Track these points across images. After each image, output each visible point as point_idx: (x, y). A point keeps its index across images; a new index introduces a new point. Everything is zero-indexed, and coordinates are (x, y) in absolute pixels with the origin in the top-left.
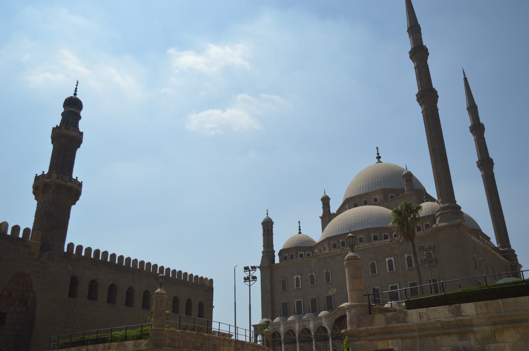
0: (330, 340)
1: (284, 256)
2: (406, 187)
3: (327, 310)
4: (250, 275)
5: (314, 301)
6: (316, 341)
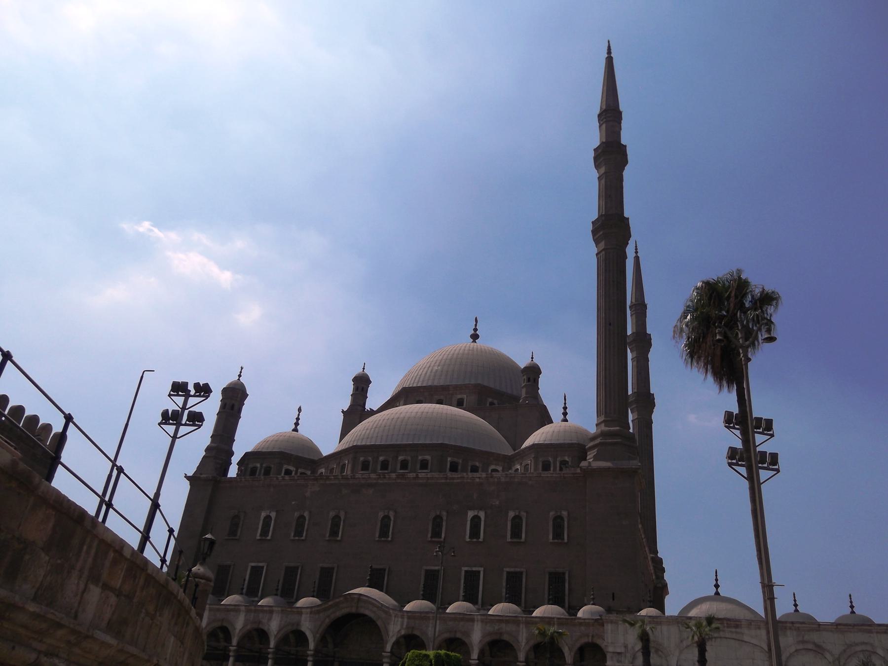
1: (251, 466)
2: (524, 391)
4: (184, 408)
5: (291, 573)
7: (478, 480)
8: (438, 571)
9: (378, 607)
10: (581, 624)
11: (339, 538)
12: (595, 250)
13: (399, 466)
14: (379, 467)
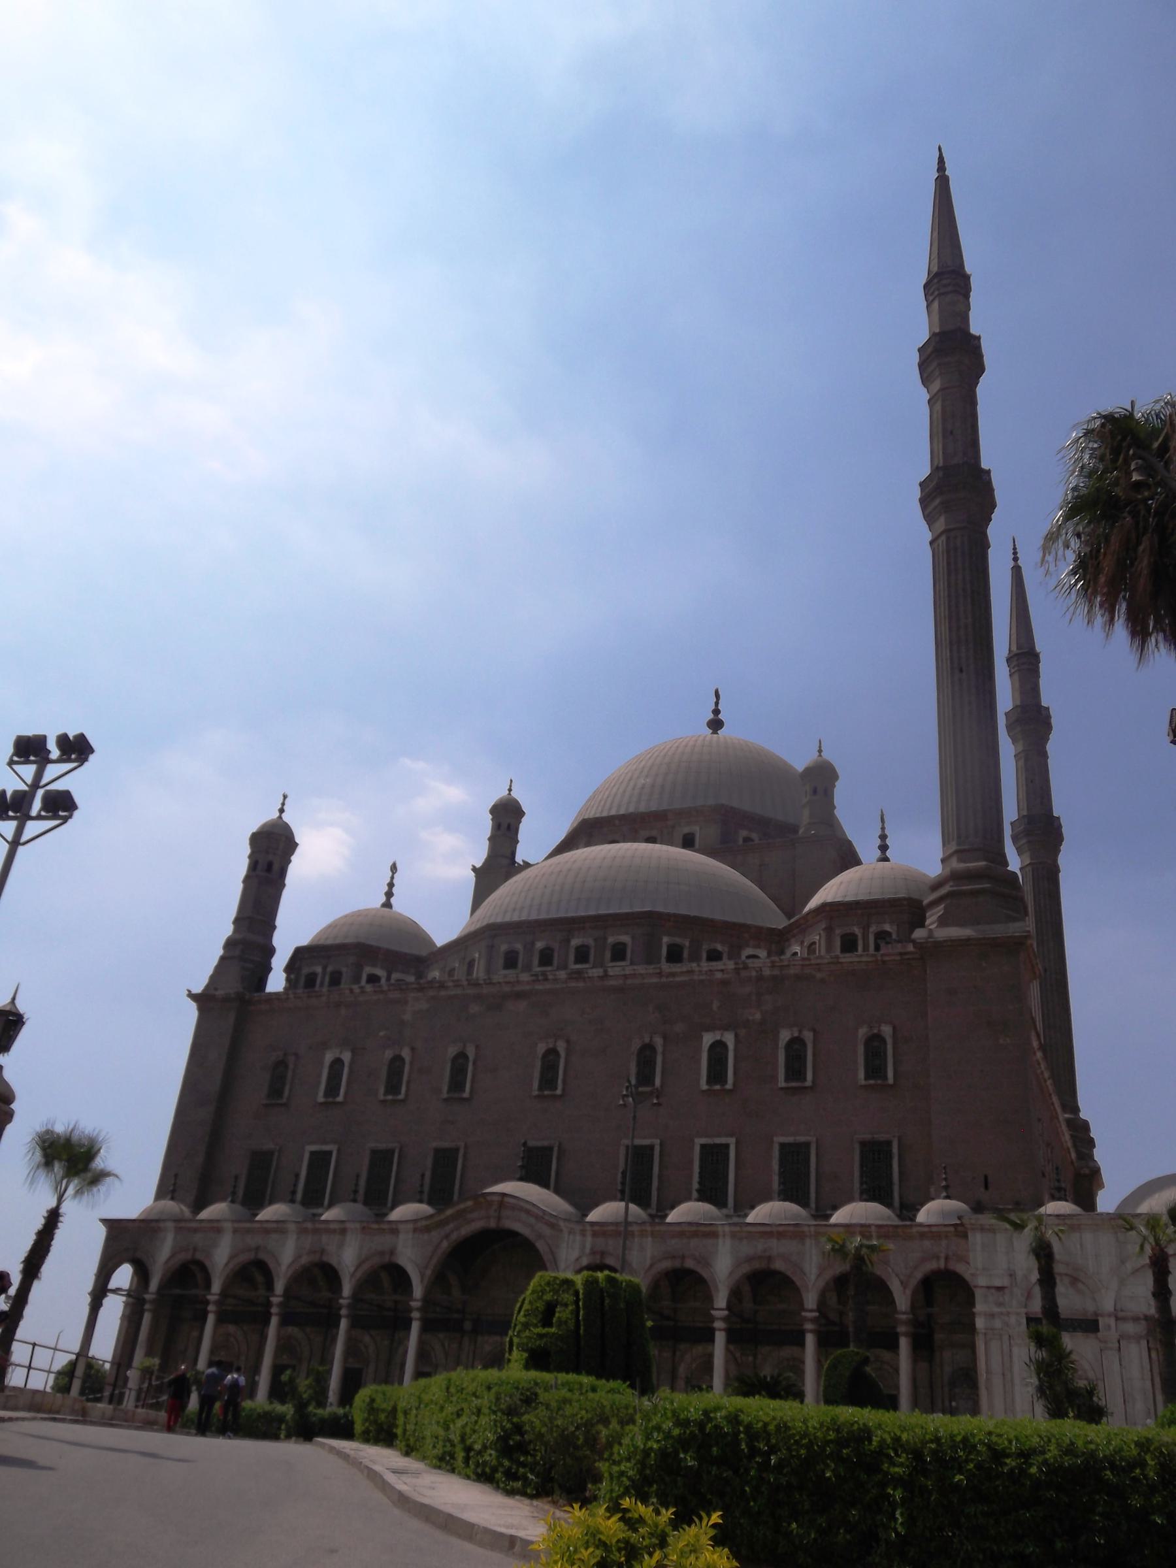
0: (415, 1327)
2: (806, 812)
3: (430, 1203)
5: (381, 1160)
6: (356, 1323)
7: (719, 975)
8: (651, 1147)
9: (536, 1217)
10: (922, 1236)
11: (466, 1095)
12: (928, 536)
13: (572, 957)
14: (536, 961)
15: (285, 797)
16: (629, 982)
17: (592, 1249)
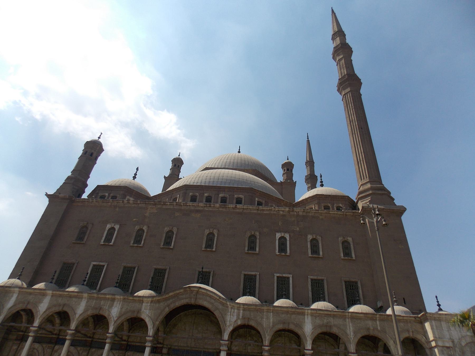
1: (100, 194)
5: (128, 271)
7: (281, 213)
9: (215, 299)
11: (172, 247)
13: (219, 200)
14: (204, 200)
15: (101, 134)
16: (245, 211)
17: (242, 317)
